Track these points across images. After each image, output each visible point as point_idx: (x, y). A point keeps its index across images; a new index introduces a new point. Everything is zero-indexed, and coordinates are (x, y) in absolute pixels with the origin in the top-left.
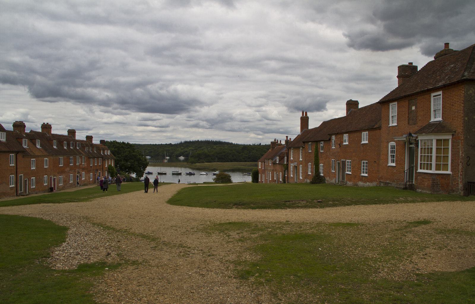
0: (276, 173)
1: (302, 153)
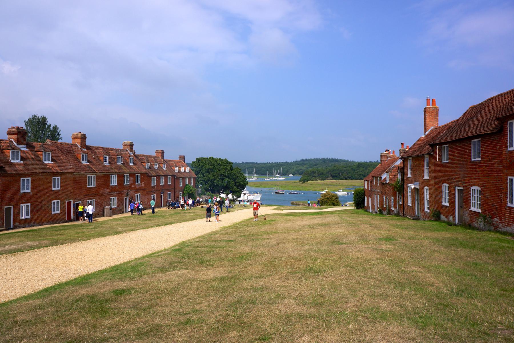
0: (386, 198)
1: (429, 165)
